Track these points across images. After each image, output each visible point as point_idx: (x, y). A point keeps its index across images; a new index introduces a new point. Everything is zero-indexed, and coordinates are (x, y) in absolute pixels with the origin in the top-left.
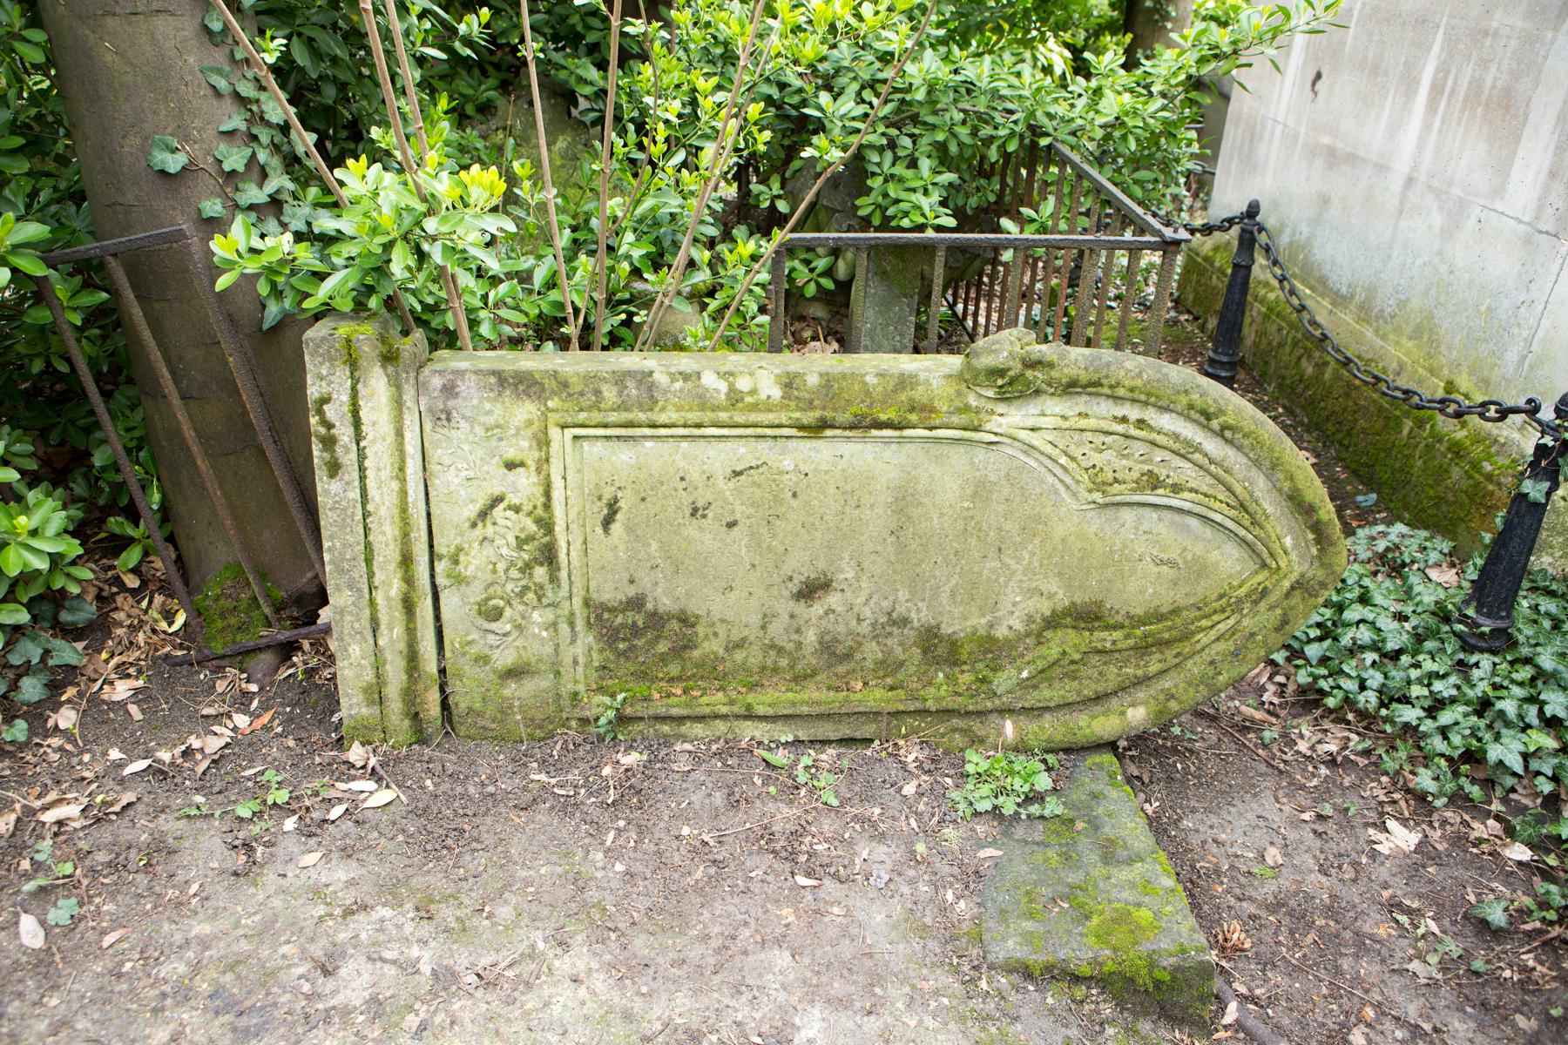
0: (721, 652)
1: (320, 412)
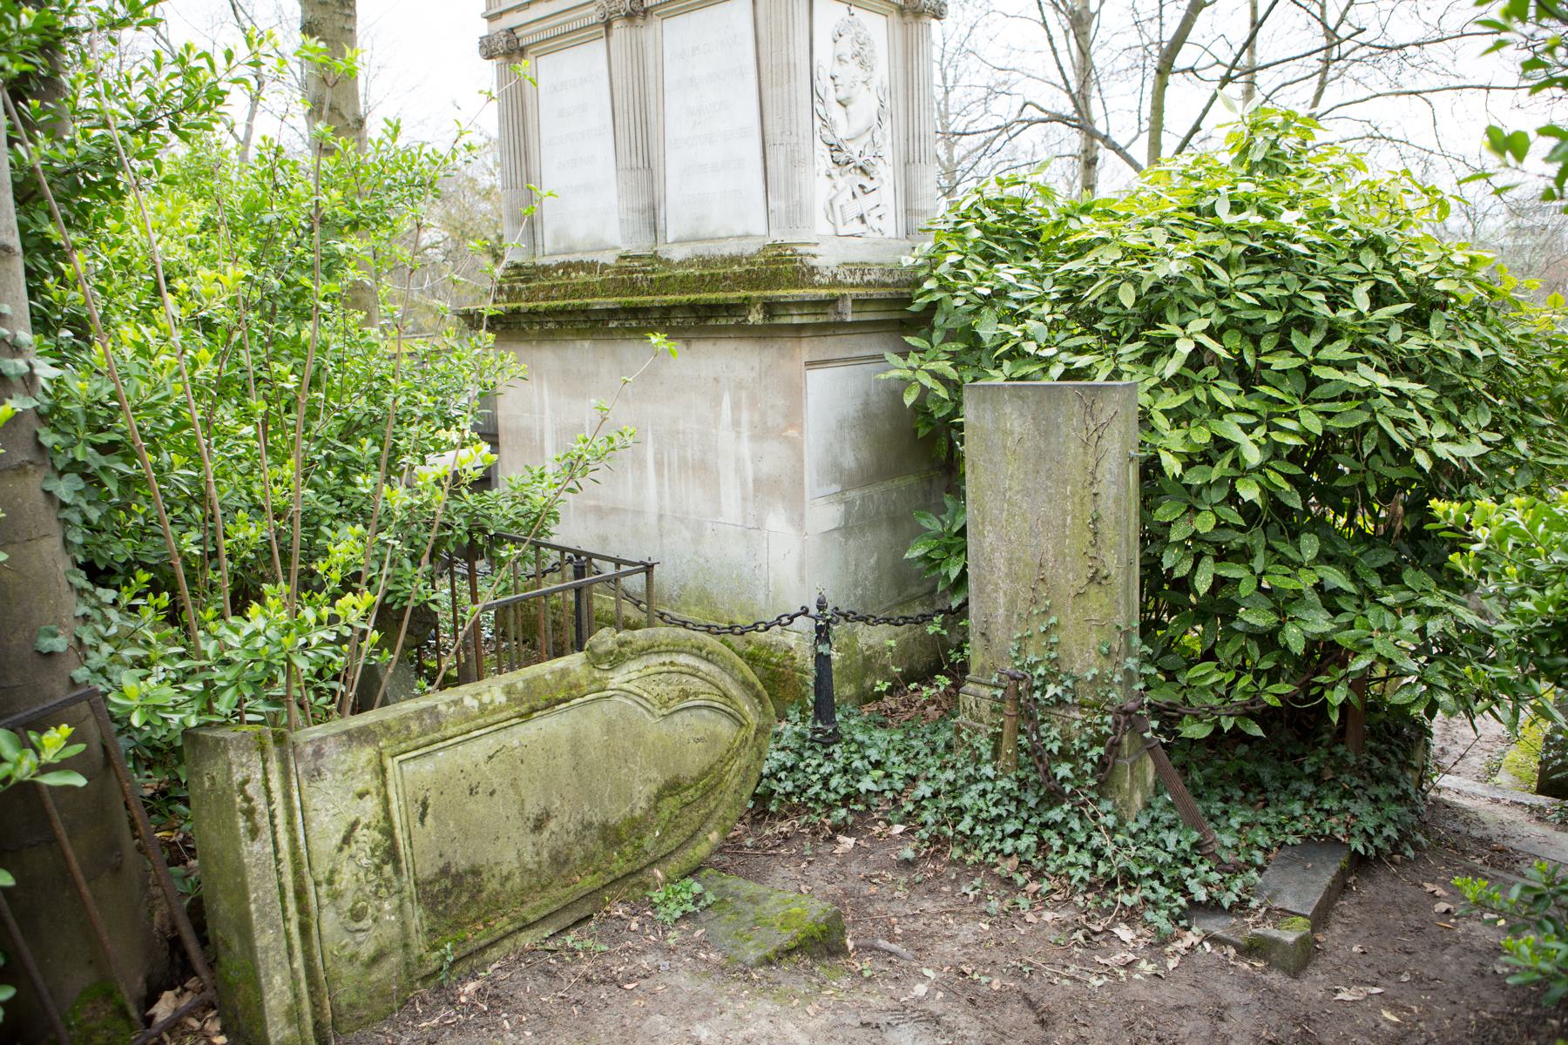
0: (498, 887)
1: (243, 791)
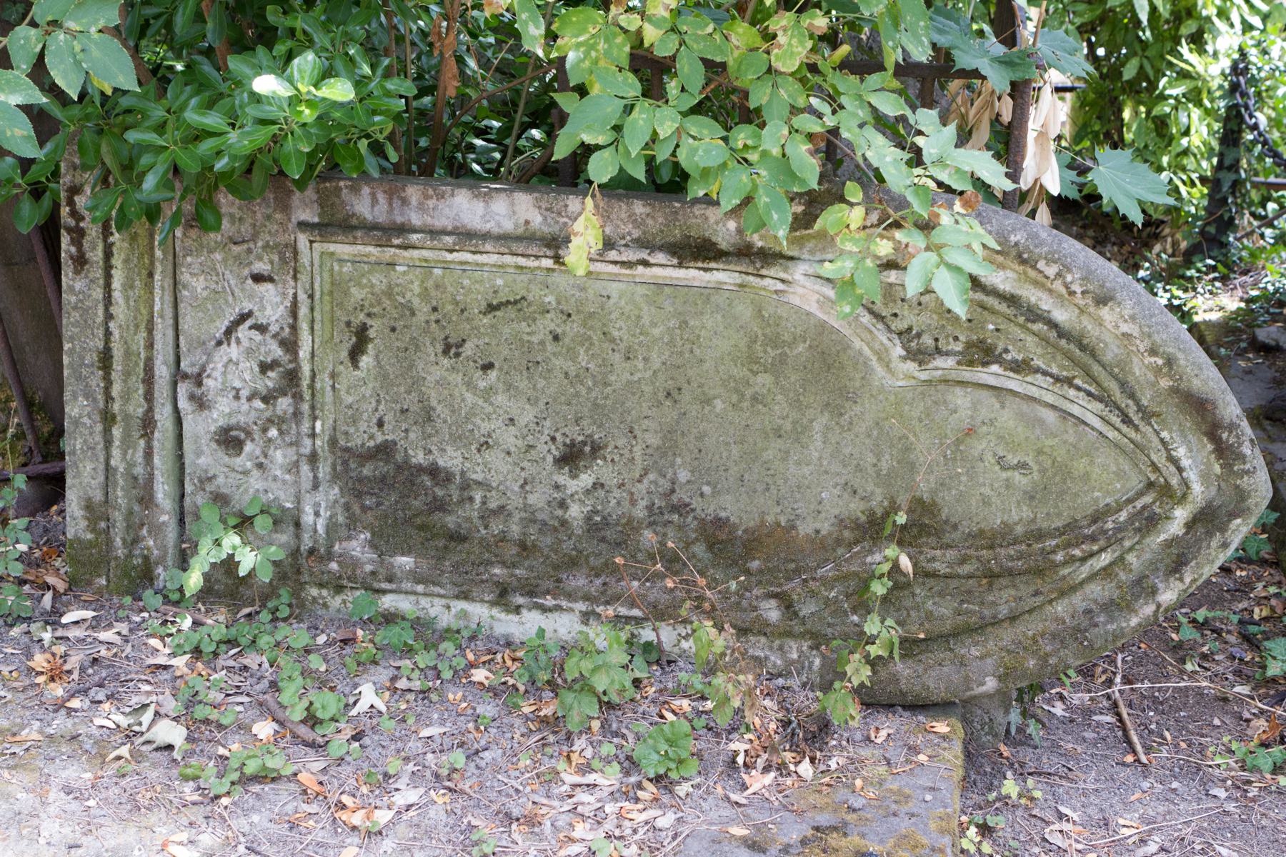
1: (71, 203)
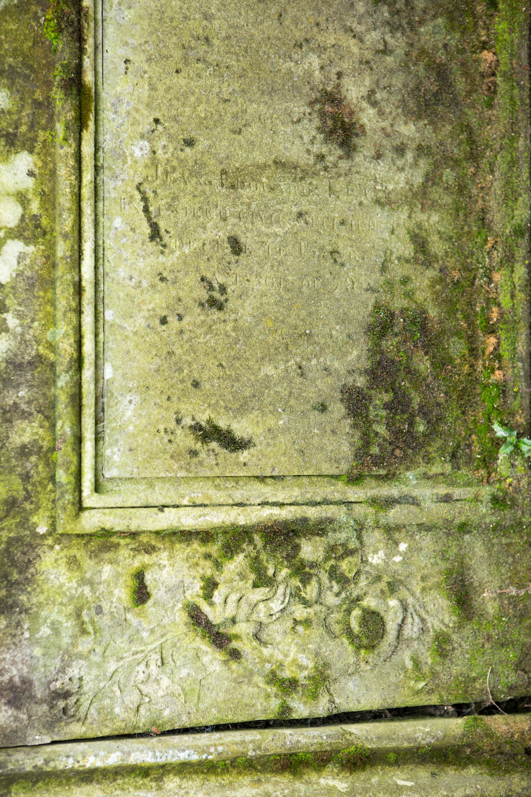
0: (431, 273)
